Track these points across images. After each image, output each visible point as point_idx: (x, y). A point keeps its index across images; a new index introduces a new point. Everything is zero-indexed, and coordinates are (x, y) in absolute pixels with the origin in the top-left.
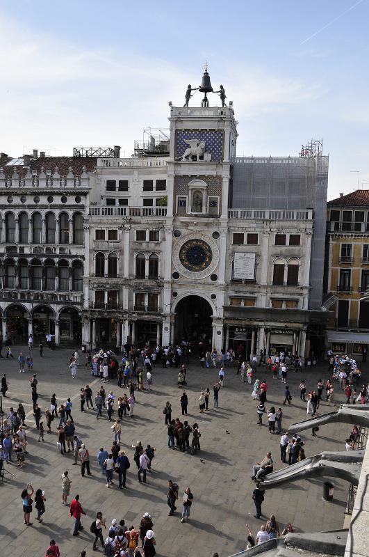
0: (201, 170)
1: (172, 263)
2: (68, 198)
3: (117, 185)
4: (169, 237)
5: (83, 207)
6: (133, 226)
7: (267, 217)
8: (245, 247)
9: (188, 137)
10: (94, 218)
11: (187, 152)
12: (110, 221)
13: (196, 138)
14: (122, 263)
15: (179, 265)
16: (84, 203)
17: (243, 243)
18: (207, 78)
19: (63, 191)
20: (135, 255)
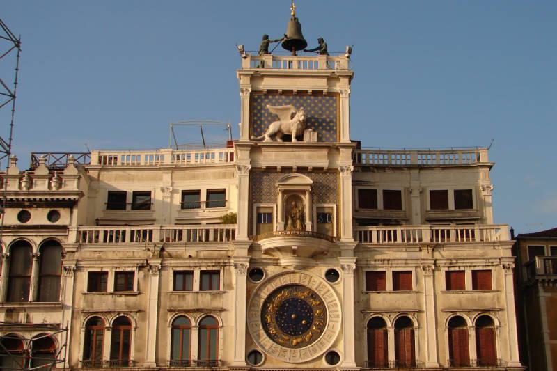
0: (299, 158)
1: (247, 333)
2: (32, 211)
3: (129, 199)
5: (65, 228)
7: (426, 238)
8: (389, 296)
10: (87, 251)
12: (120, 255)
13: (287, 104)
14: (141, 338)
16: (65, 224)
19: (25, 197)
20: (170, 317)
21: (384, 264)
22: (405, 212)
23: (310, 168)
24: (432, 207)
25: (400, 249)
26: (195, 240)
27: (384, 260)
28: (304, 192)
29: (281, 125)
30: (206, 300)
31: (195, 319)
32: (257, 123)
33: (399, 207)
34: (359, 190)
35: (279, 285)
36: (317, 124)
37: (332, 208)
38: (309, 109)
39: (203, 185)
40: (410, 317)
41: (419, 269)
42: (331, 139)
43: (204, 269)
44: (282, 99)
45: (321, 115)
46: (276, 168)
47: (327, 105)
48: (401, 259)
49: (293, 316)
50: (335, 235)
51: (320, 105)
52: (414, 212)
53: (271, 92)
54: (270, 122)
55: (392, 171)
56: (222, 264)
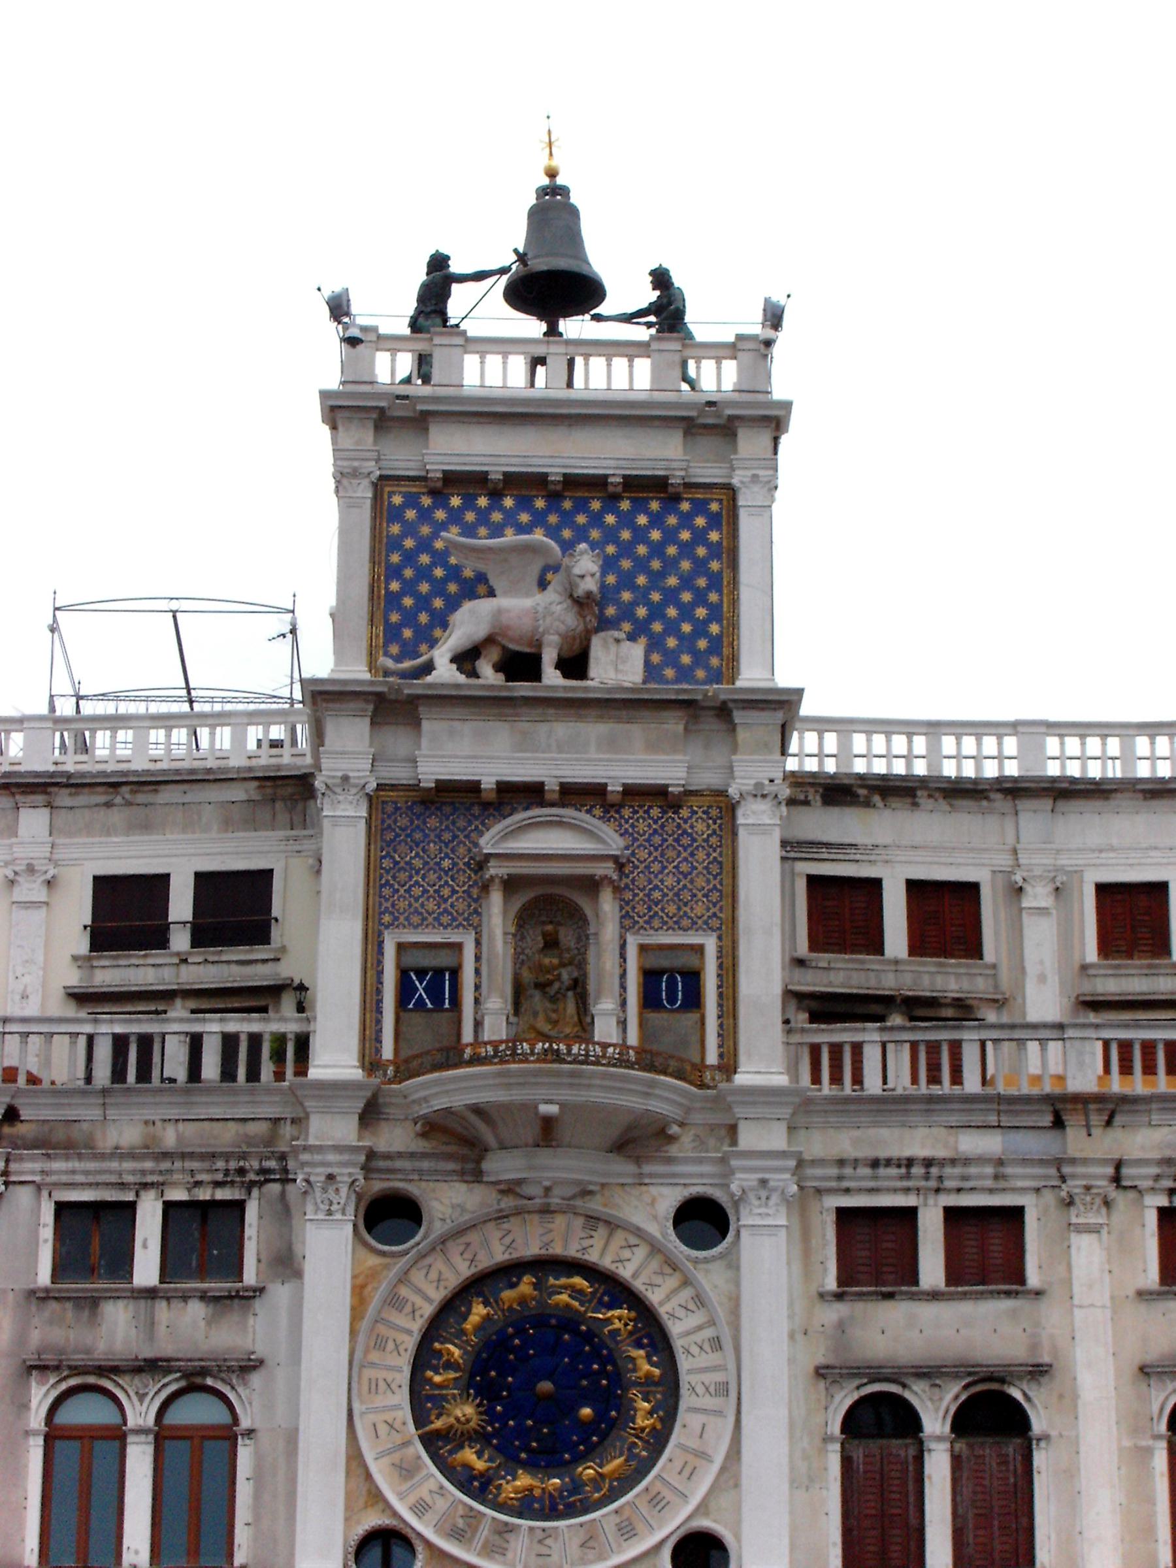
1: (355, 1456)
4: (330, 1246)
6: (29, 1167)
9: (469, 531)
11: (470, 622)
15: (406, 1471)
17: (912, 1277)
18: (553, 210)
20: (40, 1396)
21: (908, 1176)
22: (994, 966)
23: (615, 787)
24: (1106, 946)
25: (977, 1119)
26: (144, 1074)
27: (910, 1162)
28: (592, 885)
29: (499, 612)
30: (188, 1328)
31: (141, 1397)
32: (400, 608)
33: (972, 947)
34: (814, 881)
35: (485, 1262)
36: (642, 612)
37: (699, 949)
38: (611, 549)
39: (180, 857)
40: (1017, 1394)
41: (1049, 1197)
42: (700, 674)
43: (178, 1195)
44: (501, 509)
45: (663, 574)
46: (473, 787)
47: (685, 535)
48: (981, 1160)
49: (548, 1388)
50: (712, 1058)
51: (656, 535)
52: (1031, 969)
53: (454, 480)
54: (453, 604)
55: (943, 804)
56: (252, 1176)
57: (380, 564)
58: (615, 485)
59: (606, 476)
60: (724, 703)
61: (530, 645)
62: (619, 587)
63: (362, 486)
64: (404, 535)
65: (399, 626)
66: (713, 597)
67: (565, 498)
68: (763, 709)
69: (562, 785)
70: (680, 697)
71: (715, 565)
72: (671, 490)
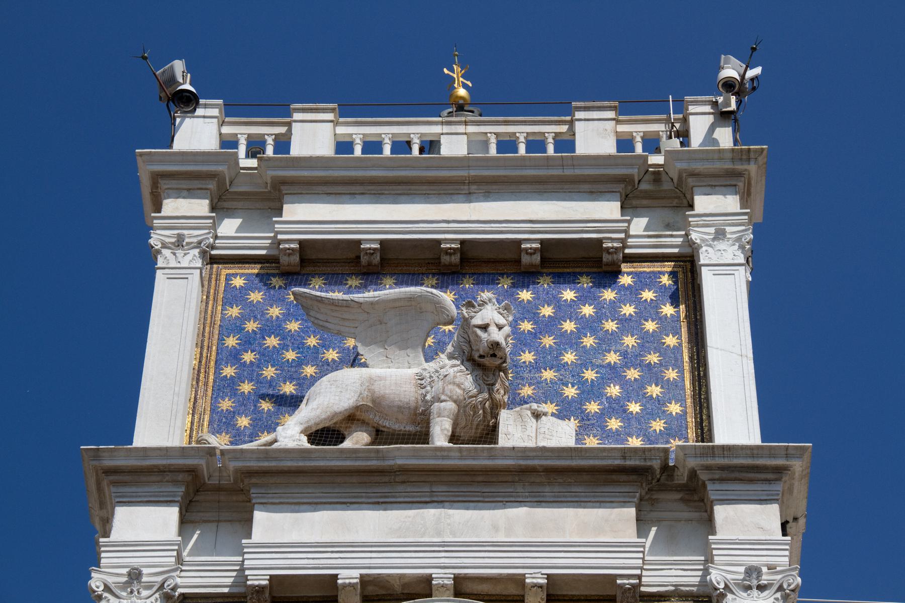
29: (371, 380)
47: (628, 310)
54: (306, 384)
57: (209, 348)
58: (531, 252)
59: (519, 242)
60: (693, 474)
61: (414, 422)
62: (537, 367)
63: (189, 257)
64: (243, 318)
65: (232, 415)
66: (672, 374)
67: (464, 275)
68: (751, 481)
69: (457, 579)
70: (629, 463)
71: (671, 341)
72: (606, 258)
